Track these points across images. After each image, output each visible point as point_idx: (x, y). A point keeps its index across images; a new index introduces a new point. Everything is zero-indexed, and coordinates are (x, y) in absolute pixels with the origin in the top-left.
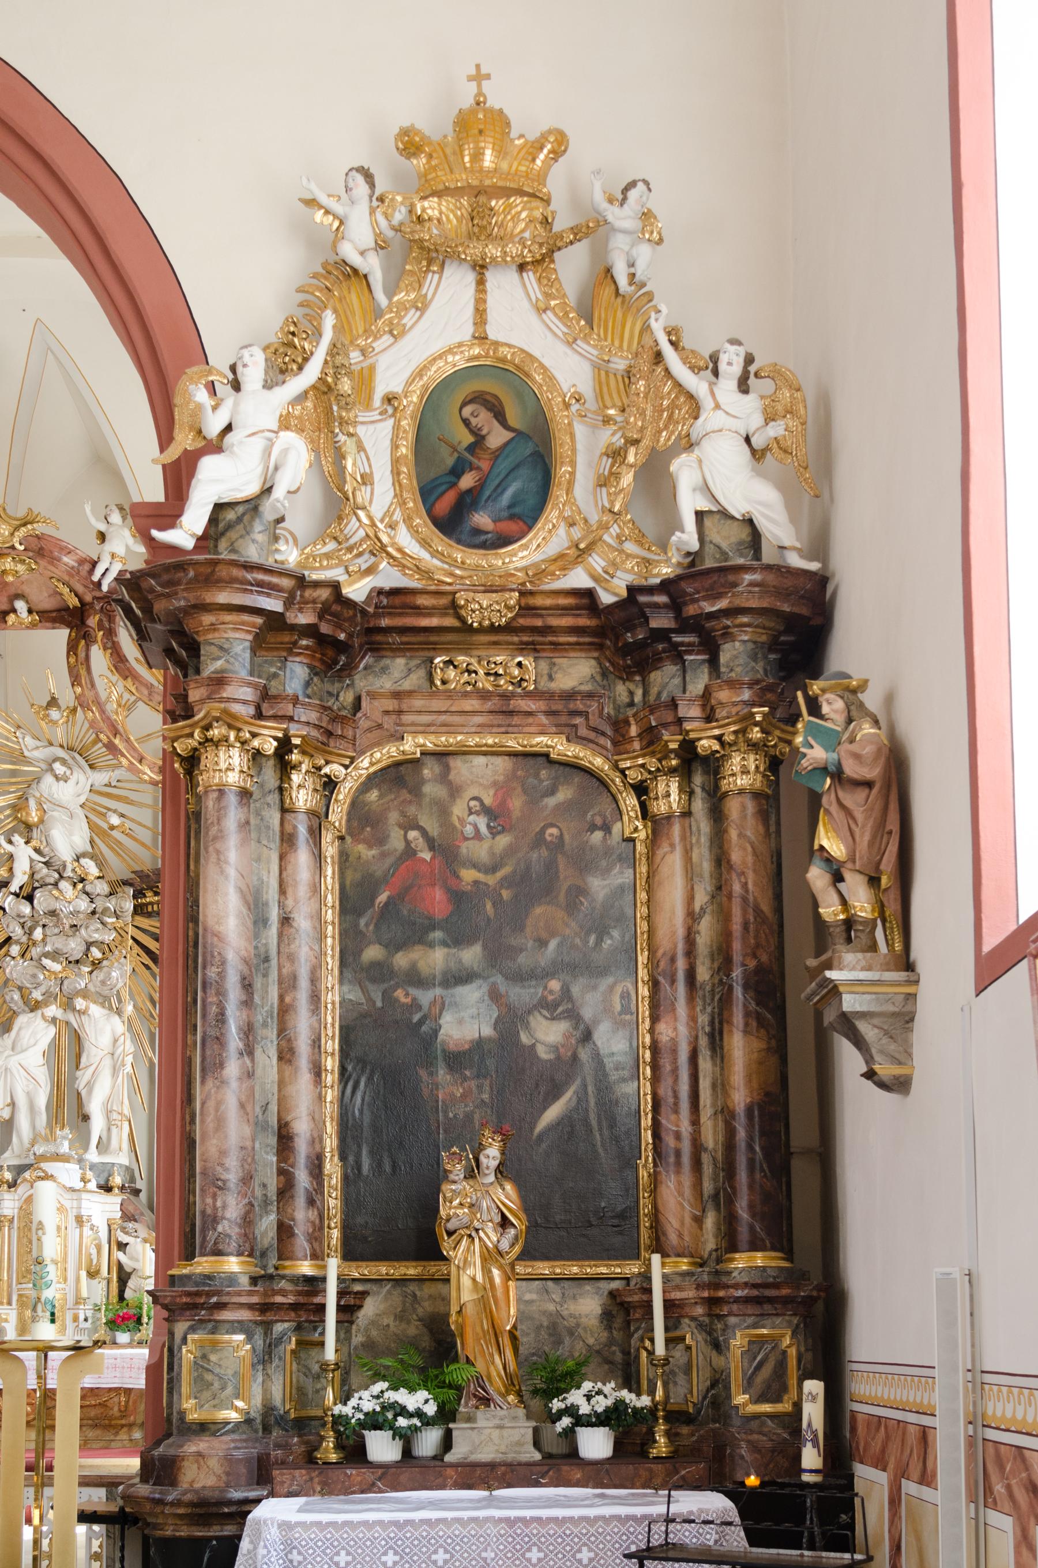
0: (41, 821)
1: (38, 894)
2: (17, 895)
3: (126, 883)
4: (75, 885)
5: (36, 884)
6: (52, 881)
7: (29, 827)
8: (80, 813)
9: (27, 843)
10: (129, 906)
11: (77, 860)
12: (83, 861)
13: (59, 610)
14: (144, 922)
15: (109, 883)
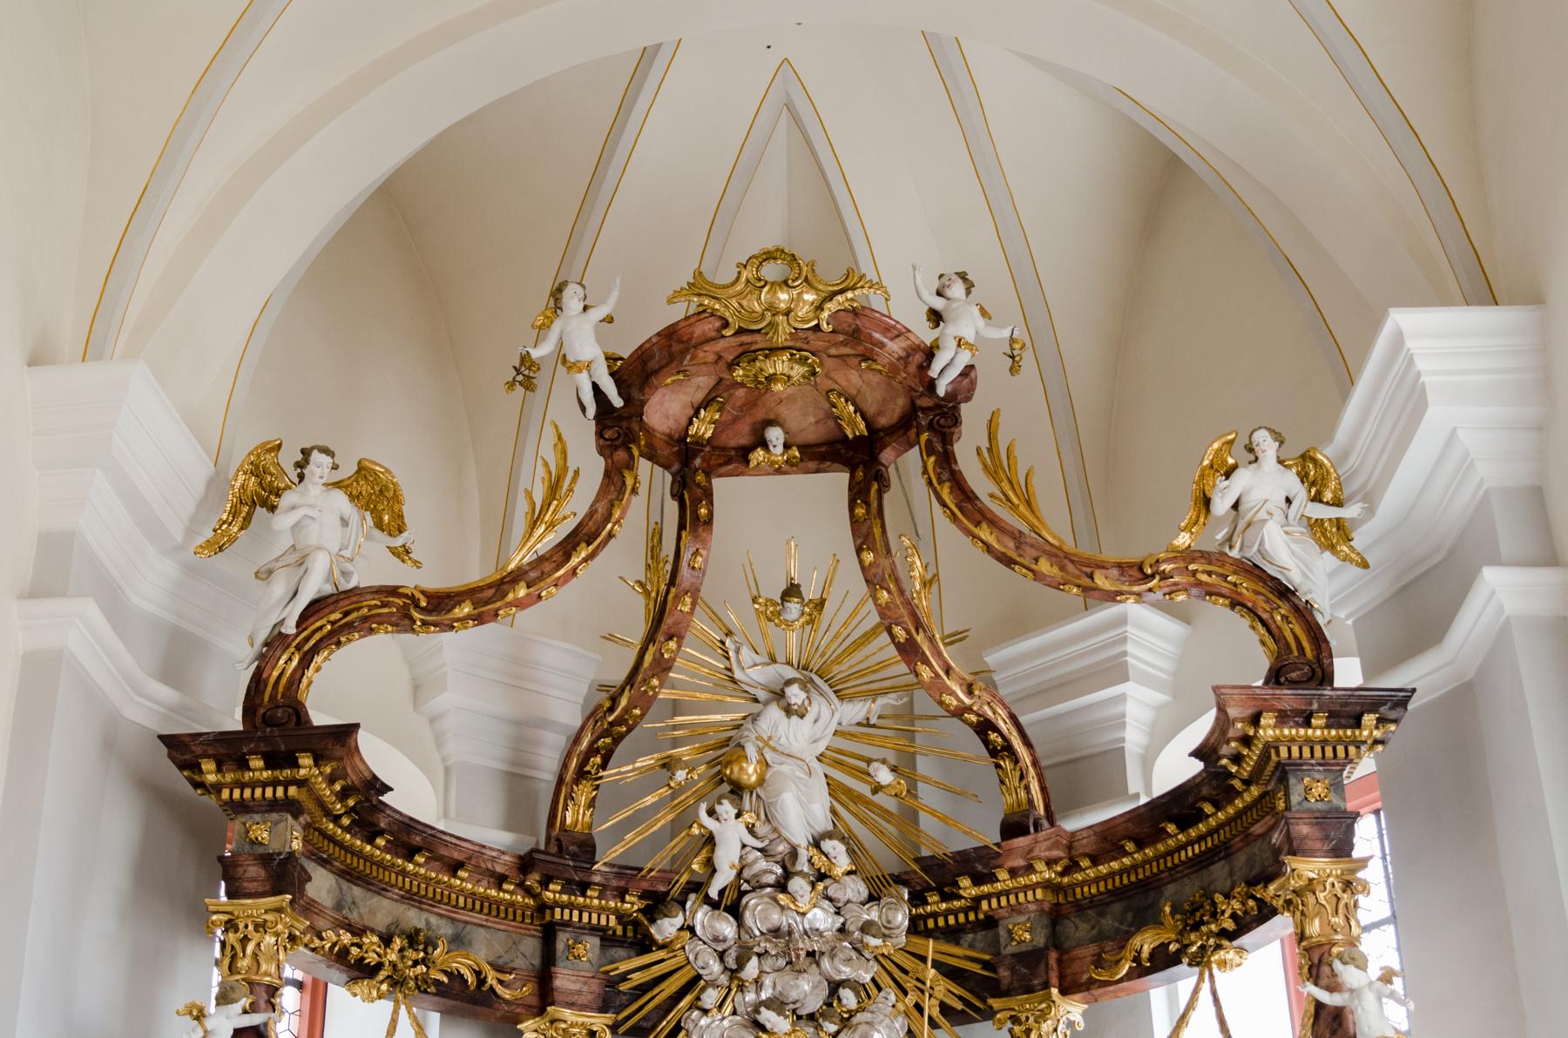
0: (761, 781)
1: (751, 901)
2: (715, 905)
3: (899, 880)
4: (813, 885)
5: (745, 887)
6: (771, 879)
7: (738, 790)
8: (815, 764)
9: (738, 816)
10: (901, 918)
11: (816, 844)
12: (827, 845)
13: (830, 443)
14: (930, 947)
15: (867, 880)
